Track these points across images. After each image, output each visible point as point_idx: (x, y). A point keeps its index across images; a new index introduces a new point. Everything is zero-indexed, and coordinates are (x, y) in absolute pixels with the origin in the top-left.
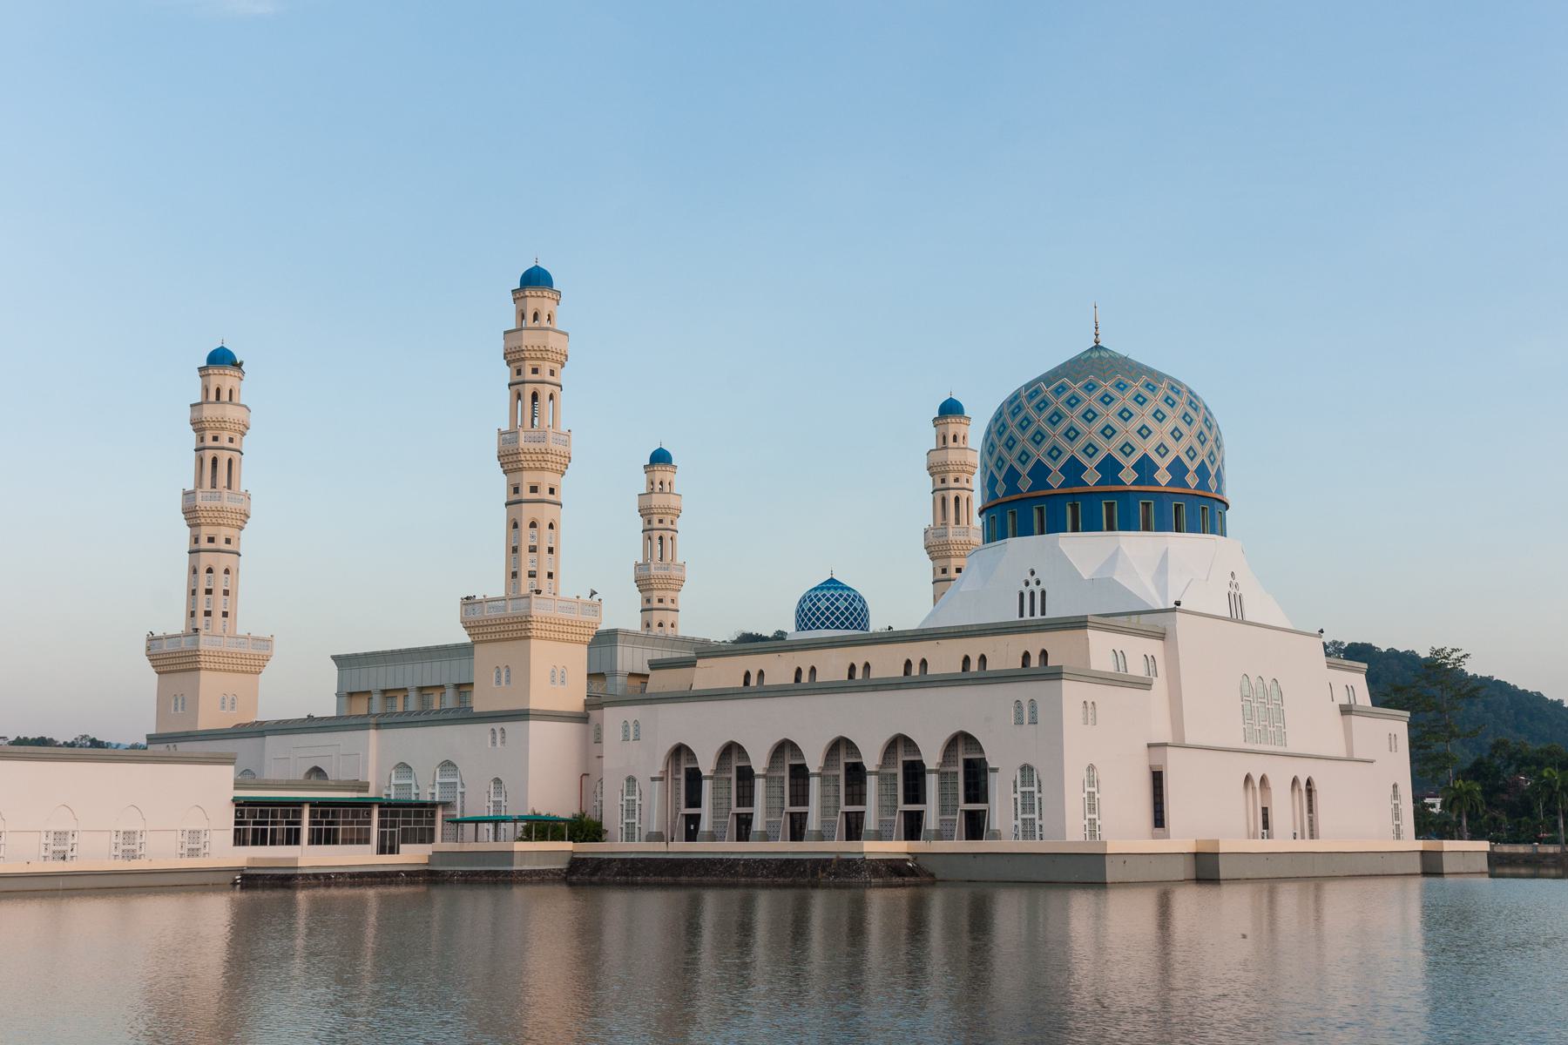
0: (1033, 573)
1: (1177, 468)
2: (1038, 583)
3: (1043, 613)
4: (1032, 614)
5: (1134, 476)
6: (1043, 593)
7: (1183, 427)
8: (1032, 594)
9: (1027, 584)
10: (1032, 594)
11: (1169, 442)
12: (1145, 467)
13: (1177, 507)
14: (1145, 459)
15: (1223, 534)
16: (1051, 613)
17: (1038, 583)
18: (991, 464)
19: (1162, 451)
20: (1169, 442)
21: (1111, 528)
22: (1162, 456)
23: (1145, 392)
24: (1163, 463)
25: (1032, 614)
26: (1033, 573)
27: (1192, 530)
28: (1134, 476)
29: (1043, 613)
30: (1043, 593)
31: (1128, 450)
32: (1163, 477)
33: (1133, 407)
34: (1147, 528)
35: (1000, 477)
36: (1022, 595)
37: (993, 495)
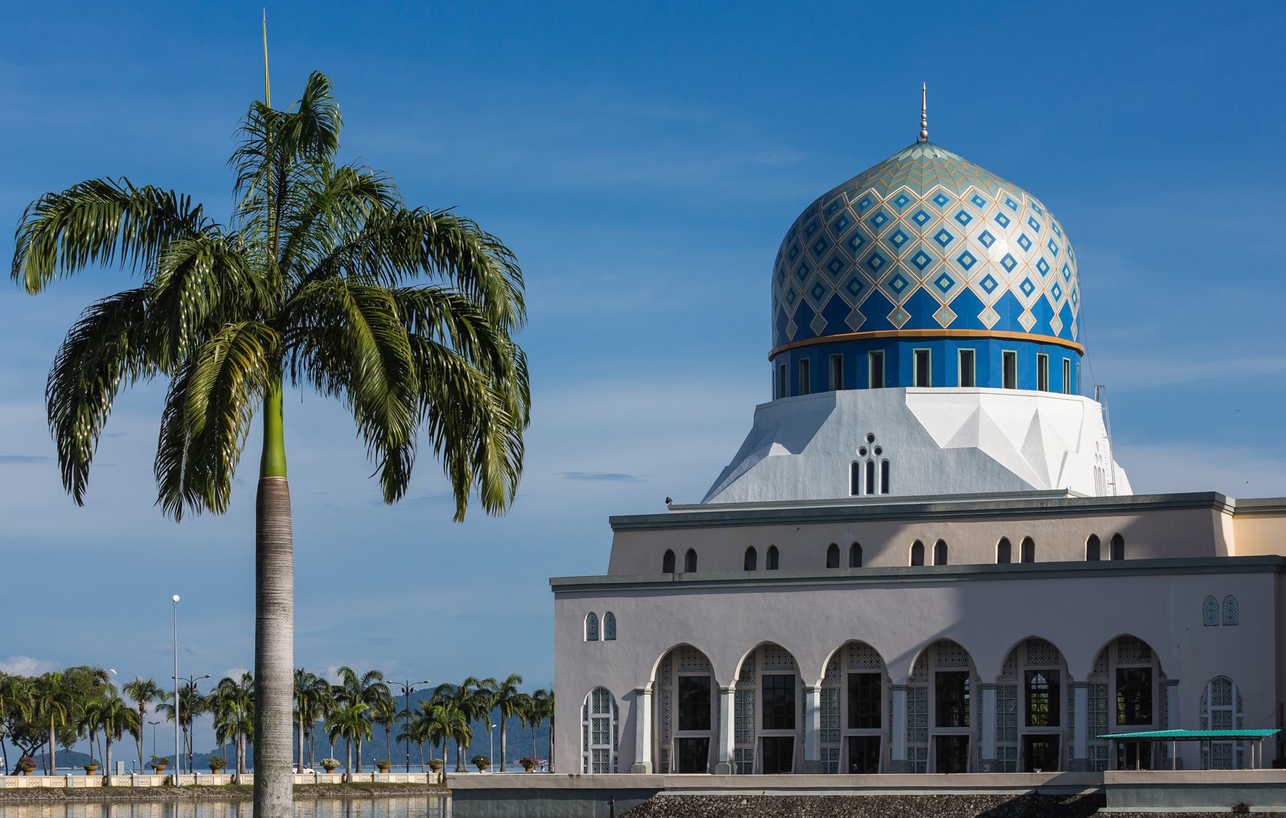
0: (871, 438)
1: (1043, 309)
2: (878, 451)
3: (885, 489)
4: (870, 489)
5: (996, 318)
6: (886, 465)
7: (1050, 259)
8: (871, 466)
9: (863, 452)
10: (871, 466)
11: (1035, 277)
12: (1009, 306)
13: (1041, 358)
14: (967, 293)
15: (1074, 390)
16: (896, 490)
17: (878, 451)
18: (803, 293)
19: (1027, 287)
20: (1035, 277)
21: (967, 383)
22: (989, 291)
23: (971, 209)
24: (1028, 302)
25: (870, 489)
26: (871, 438)
27: (1056, 388)
28: (996, 318)
29: (885, 489)
30: (886, 465)
31: (989, 284)
32: (1027, 320)
33: (994, 229)
34: (1009, 384)
35: (818, 308)
36: (855, 467)
37: (804, 331)
